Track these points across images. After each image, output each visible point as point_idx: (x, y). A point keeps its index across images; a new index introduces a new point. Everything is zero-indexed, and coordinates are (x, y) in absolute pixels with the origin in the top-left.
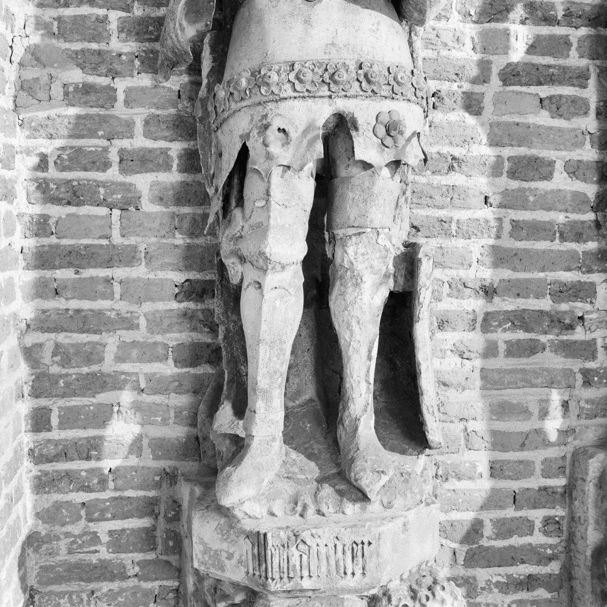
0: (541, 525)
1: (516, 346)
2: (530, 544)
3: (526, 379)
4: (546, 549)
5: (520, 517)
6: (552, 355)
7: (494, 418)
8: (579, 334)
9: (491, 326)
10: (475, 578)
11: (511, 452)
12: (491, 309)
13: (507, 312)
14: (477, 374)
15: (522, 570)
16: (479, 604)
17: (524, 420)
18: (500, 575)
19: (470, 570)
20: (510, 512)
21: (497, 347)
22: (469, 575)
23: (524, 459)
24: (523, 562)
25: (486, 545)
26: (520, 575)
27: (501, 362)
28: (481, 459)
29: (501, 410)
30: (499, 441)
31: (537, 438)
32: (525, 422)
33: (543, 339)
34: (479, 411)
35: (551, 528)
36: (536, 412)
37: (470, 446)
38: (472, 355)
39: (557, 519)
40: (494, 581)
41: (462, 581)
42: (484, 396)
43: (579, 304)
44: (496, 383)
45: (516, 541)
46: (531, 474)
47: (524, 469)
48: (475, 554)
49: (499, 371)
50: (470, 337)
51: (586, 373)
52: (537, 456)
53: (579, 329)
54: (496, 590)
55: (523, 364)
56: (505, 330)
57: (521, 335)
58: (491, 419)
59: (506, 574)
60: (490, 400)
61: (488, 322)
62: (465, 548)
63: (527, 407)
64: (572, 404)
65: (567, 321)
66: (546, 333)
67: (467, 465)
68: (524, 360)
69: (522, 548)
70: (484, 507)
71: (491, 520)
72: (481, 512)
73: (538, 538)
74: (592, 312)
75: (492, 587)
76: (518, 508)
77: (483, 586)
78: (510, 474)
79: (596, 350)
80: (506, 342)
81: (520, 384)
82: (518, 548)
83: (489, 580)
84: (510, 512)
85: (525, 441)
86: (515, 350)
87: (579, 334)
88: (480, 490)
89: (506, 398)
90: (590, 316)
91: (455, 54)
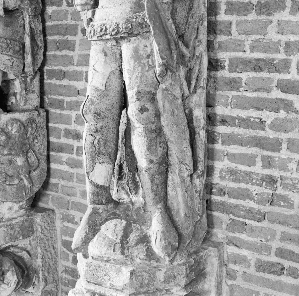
9: (80, 153)
67: (71, 216)
91: (65, 22)
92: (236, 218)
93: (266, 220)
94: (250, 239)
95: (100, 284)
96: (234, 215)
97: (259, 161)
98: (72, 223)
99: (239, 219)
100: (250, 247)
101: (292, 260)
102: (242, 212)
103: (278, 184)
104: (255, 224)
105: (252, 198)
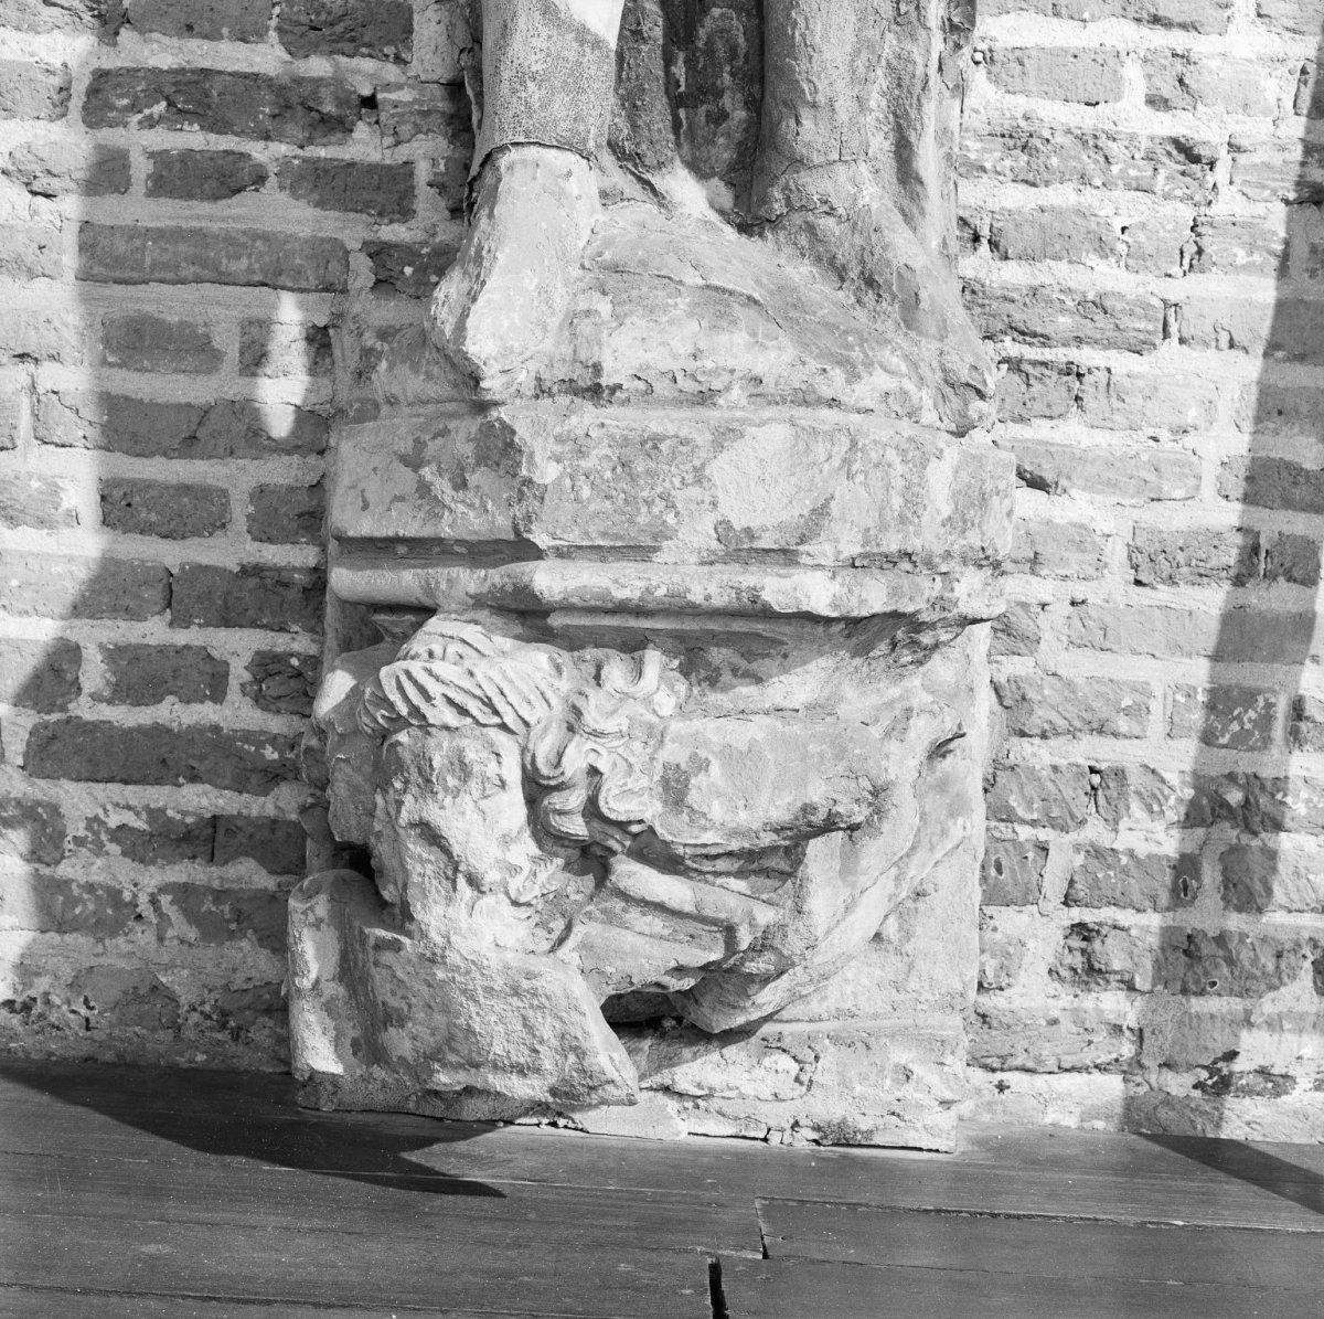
0: (247, 676)
1: (178, 165)
2: (216, 729)
3: (204, 261)
4: (260, 745)
5: (187, 647)
6: (284, 197)
7: (111, 359)
8: (364, 145)
9: (112, 108)
10: (54, 809)
11: (158, 460)
12: (110, 61)
13: (156, 72)
14: (70, 238)
15: (195, 800)
16: (68, 882)
17: (197, 371)
18: (129, 808)
19: (42, 783)
20: (155, 631)
21: (126, 167)
22: (39, 796)
23: (198, 480)
24: (194, 778)
25: (88, 716)
26: (185, 813)
27: (138, 209)
28: (77, 475)
29: (131, 341)
30: (123, 426)
31: (238, 428)
32: (201, 379)
33: (260, 152)
34: (71, 337)
35: (271, 688)
36: (232, 351)
37: (42, 432)
38: (55, 184)
39: (295, 662)
40: (114, 821)
41: (16, 812)
42: (85, 299)
43: (368, 65)
44: (119, 262)
45: (172, 713)
46: (220, 524)
47: (193, 513)
48: (54, 737)
49: (133, 233)
50: (53, 137)
51: (378, 252)
52: (237, 477)
53: (362, 131)
54: (114, 849)
55: (198, 218)
56: (150, 123)
57: (194, 138)
58: (104, 362)
59: (147, 808)
60: (101, 311)
61: (101, 97)
62: (29, 719)
63: (207, 336)
64: (343, 342)
65: (329, 108)
66: (267, 138)
67: (35, 484)
68: (205, 208)
69: (196, 732)
70: (82, 608)
71: (101, 647)
72: (76, 622)
73: (236, 713)
74: (400, 87)
75: (104, 837)
76: (181, 621)
77: (81, 833)
78: (153, 517)
79: (409, 193)
80: (152, 155)
81: (189, 271)
82: (179, 735)
83: (96, 818)
84: (155, 631)
85: (196, 432)
86: (175, 177)
87: (364, 145)
88: (70, 559)
89: (149, 308)
90: (393, 96)
92: (1032, 353)
93: (1174, 340)
94: (1102, 438)
95: (640, 552)
96: (1024, 334)
97: (1133, 72)
98: (42, 523)
99: (1047, 354)
100: (1108, 478)
101: (1288, 504)
102: (1061, 319)
103: (1221, 174)
104: (1122, 362)
105: (1102, 247)
